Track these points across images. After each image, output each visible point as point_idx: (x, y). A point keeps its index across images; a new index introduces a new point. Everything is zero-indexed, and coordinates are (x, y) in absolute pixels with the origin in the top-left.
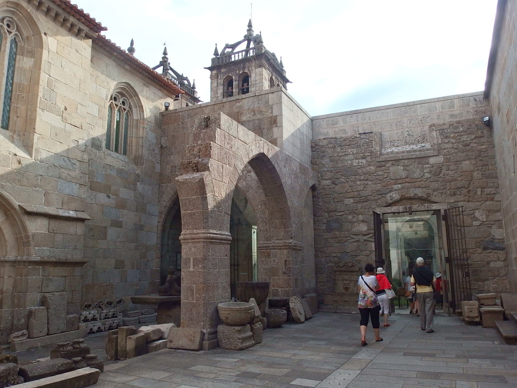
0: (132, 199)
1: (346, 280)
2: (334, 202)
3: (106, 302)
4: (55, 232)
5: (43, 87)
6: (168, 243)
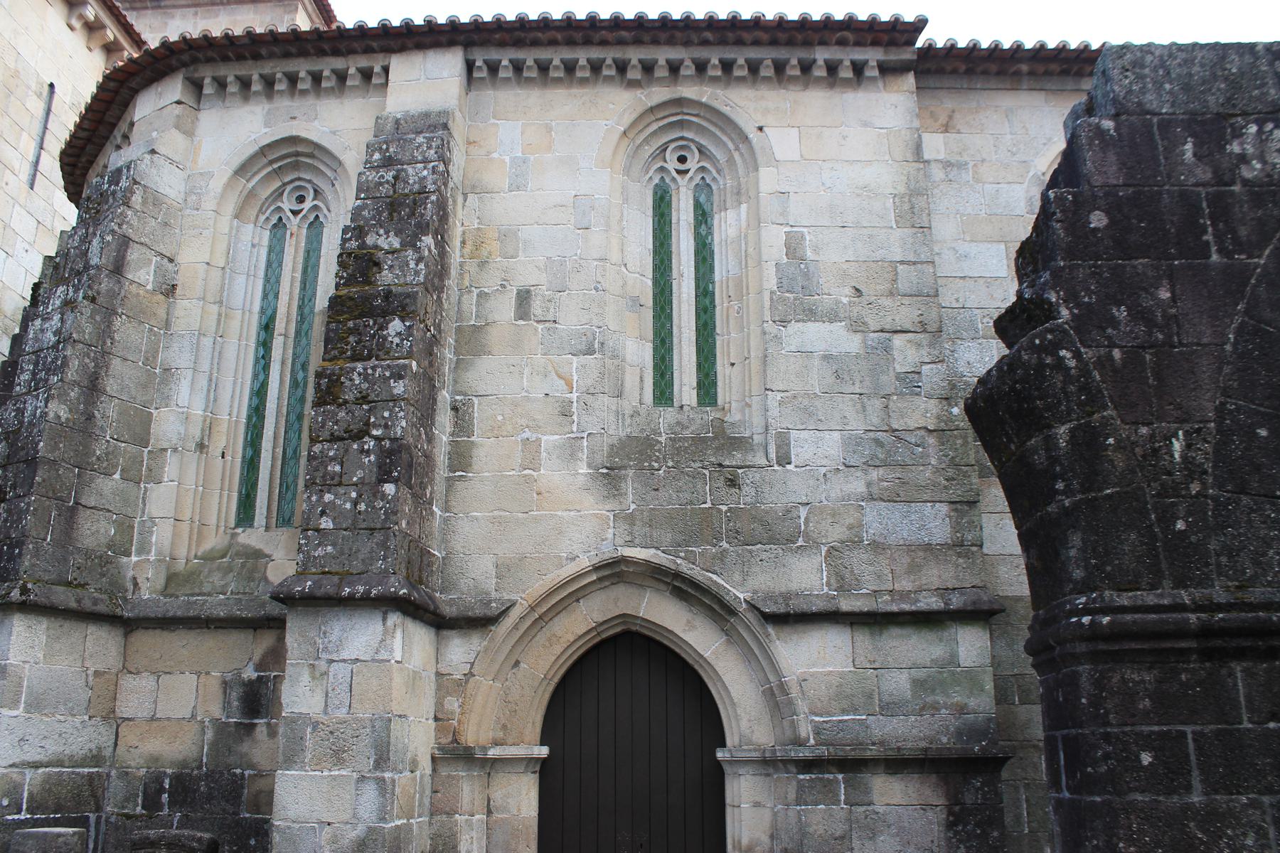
5: (774, 263)
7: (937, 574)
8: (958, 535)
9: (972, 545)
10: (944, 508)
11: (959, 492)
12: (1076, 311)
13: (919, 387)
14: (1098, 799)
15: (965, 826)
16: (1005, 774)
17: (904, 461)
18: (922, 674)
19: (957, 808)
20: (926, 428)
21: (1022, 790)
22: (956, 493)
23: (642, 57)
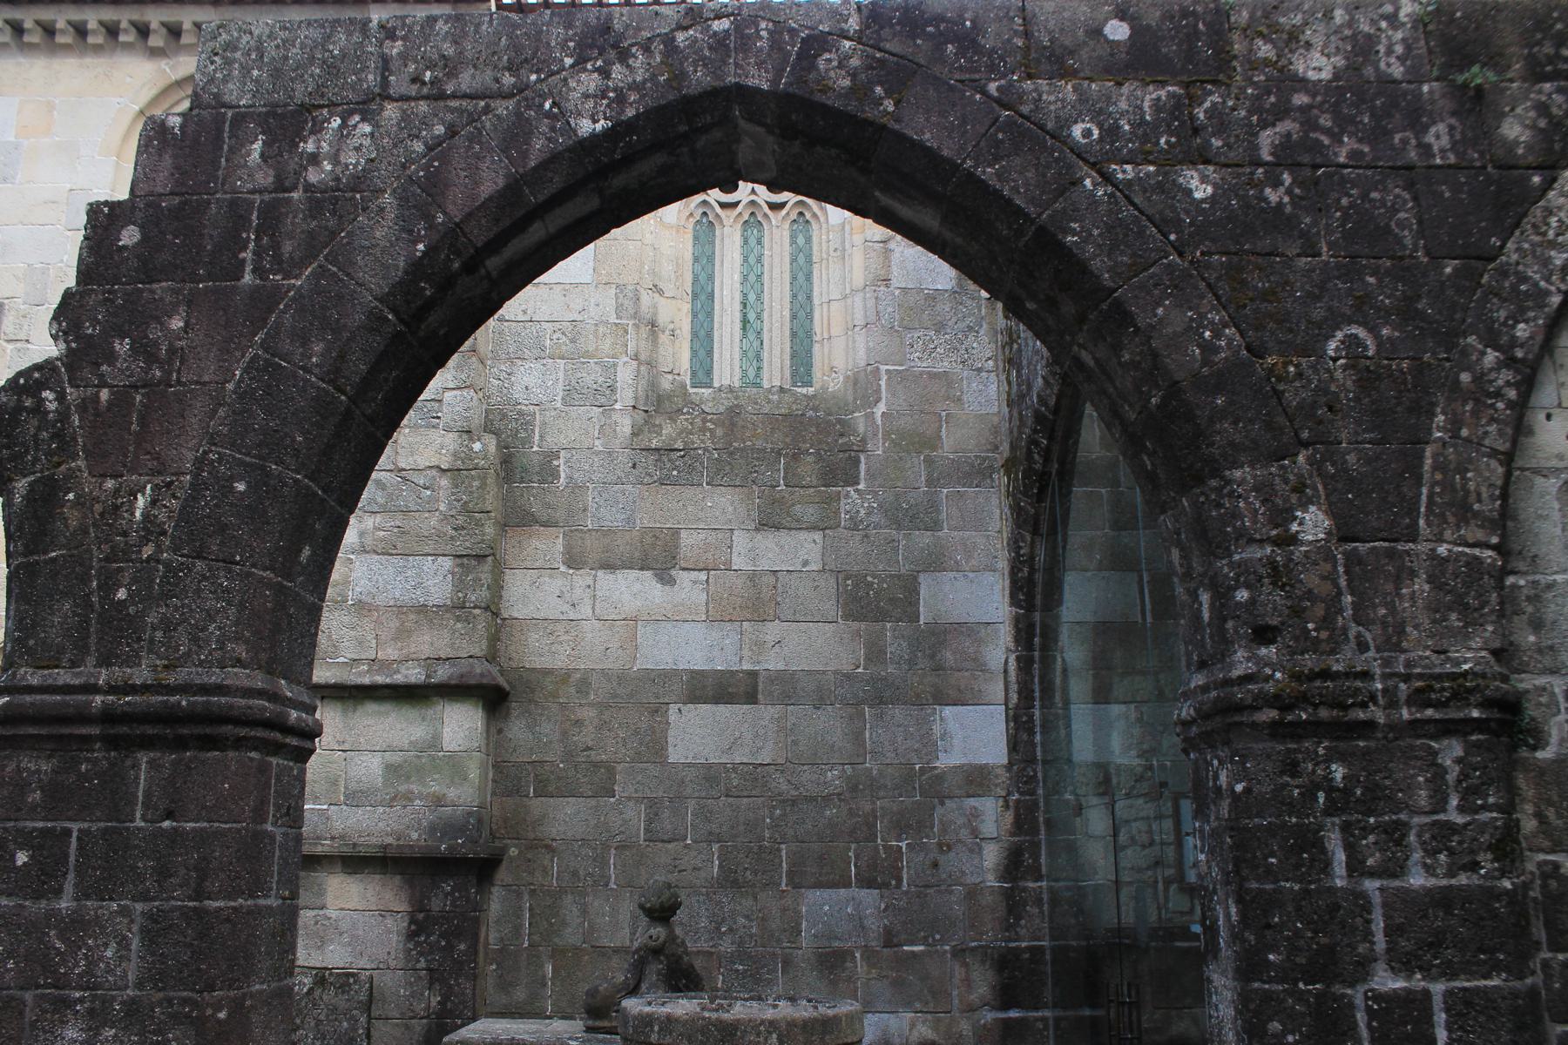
4: (346, 747)
8: (460, 595)
9: (474, 608)
10: (447, 563)
11: (468, 544)
12: (74, 345)
13: (439, 418)
15: (428, 937)
18: (395, 758)
19: (421, 916)
20: (438, 467)
21: (526, 897)
22: (463, 545)
23: (165, 19)
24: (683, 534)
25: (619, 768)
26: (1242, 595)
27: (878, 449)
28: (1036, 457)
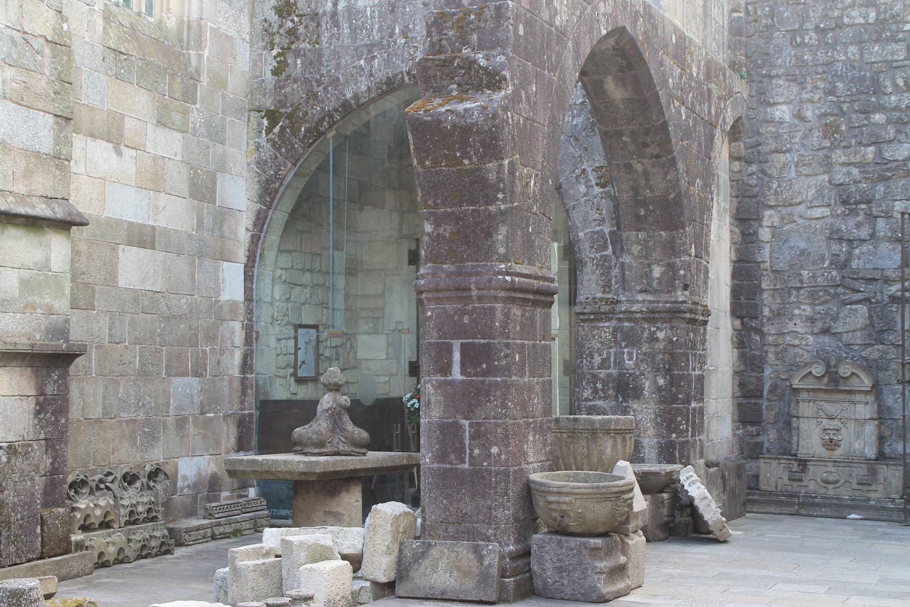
0: (179, 158)
1: (831, 418)
2: (799, 174)
3: (119, 476)
6: (272, 297)
7: (43, 183)
9: (65, 160)
10: (50, 119)
14: (499, 379)
15: (45, 415)
16: (72, 368)
17: (29, 66)
18: (26, 274)
19: (41, 398)
22: (58, 108)
24: (127, 119)
25: (97, 288)
26: (682, 272)
27: (205, 80)
28: (325, 123)
